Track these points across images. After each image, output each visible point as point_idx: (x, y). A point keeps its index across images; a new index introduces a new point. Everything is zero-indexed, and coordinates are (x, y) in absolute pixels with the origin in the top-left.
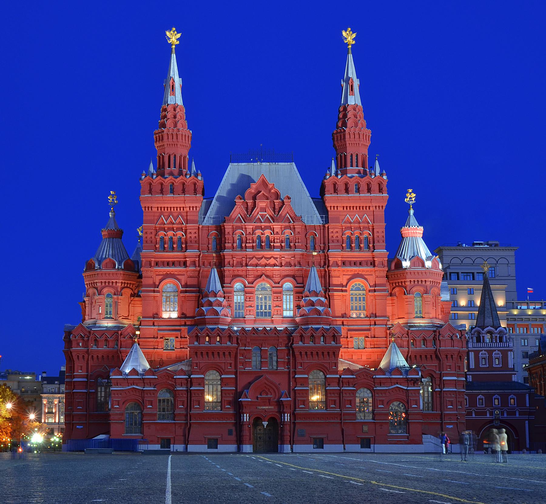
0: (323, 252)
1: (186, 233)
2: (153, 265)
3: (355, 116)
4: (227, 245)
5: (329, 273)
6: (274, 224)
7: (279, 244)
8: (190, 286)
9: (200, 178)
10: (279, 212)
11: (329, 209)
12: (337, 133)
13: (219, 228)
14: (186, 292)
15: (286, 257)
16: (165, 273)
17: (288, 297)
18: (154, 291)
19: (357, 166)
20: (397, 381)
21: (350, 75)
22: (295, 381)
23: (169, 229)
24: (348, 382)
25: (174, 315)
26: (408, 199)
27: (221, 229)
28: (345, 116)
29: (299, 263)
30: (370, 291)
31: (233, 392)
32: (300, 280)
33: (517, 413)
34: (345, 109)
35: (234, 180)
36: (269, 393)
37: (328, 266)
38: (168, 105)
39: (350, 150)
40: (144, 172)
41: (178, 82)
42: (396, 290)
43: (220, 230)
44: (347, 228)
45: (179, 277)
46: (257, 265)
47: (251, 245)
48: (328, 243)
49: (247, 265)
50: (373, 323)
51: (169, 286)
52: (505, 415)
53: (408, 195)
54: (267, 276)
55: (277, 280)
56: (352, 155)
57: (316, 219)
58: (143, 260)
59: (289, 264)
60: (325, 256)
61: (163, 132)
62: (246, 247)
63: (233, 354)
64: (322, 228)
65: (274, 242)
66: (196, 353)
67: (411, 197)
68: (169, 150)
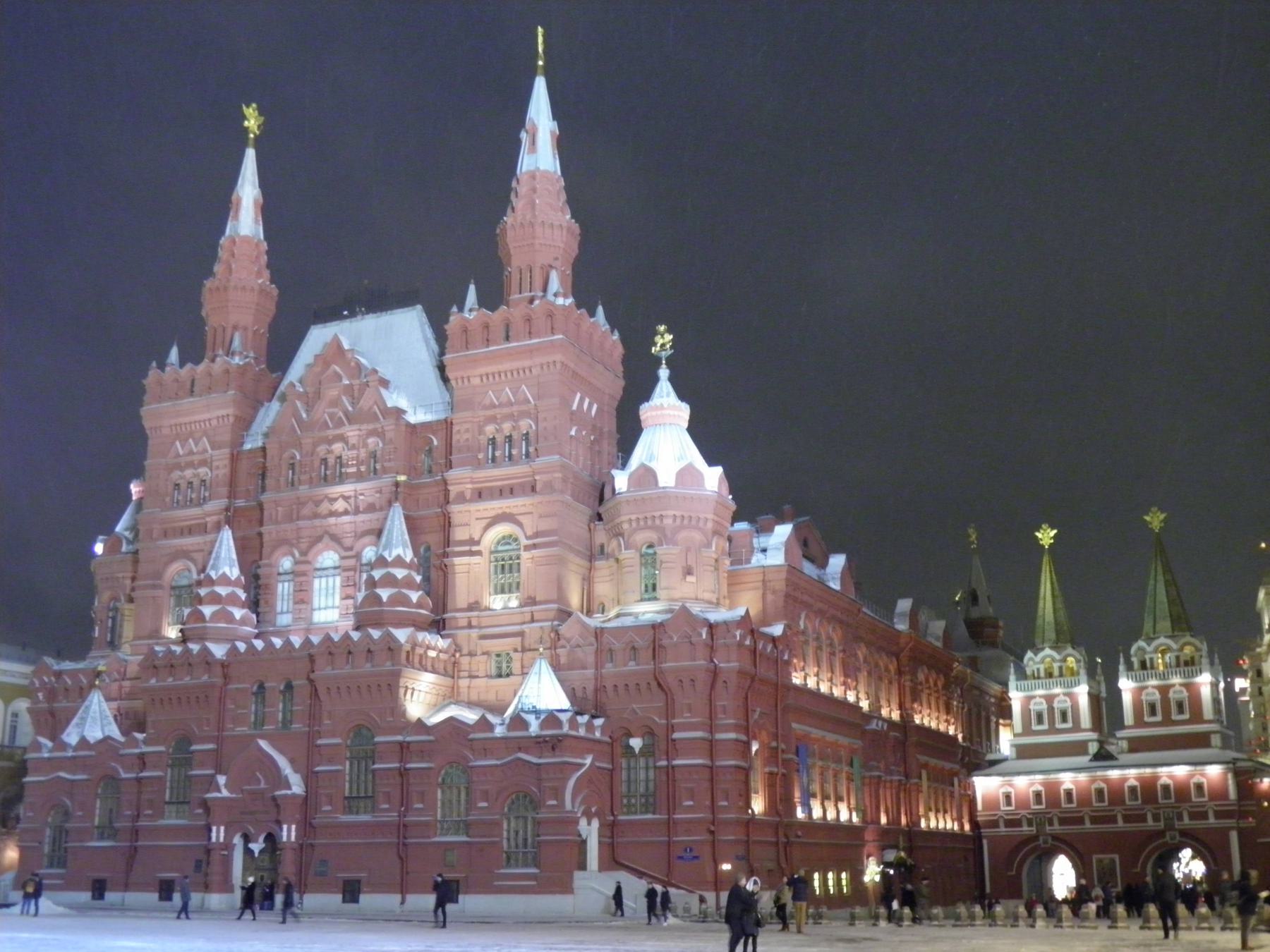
7: (353, 470)
15: (367, 493)
24: (424, 751)
30: (527, 548)
33: (1211, 814)
35: (310, 360)
45: (195, 555)
50: (528, 617)
52: (1186, 820)
53: (659, 340)
54: (336, 539)
55: (348, 542)
59: (371, 508)
67: (664, 340)
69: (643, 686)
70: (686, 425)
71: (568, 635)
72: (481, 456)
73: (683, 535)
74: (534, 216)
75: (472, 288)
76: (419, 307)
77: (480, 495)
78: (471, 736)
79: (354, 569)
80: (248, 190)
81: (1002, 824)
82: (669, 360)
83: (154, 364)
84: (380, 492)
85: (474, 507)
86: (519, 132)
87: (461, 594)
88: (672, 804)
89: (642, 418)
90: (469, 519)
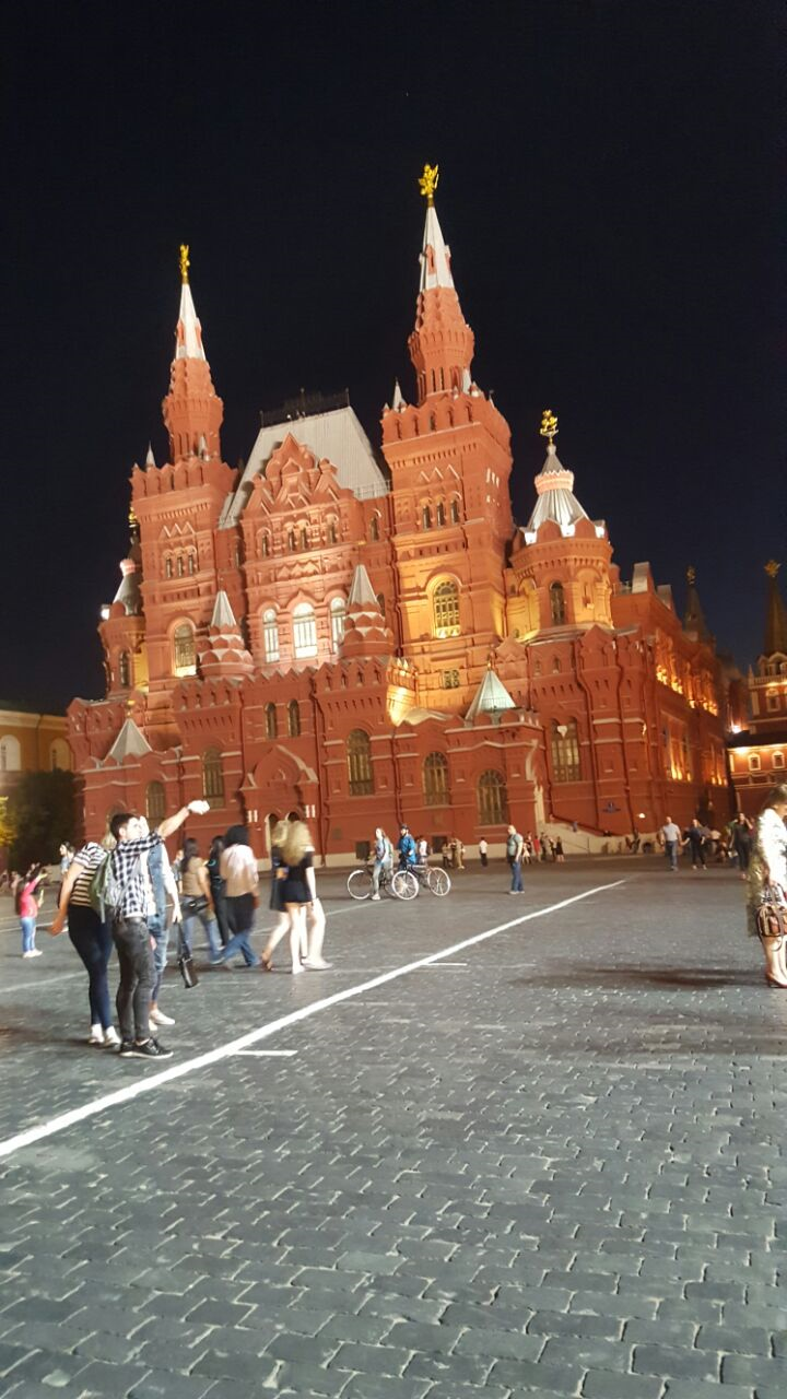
2: (157, 599)
5: (398, 572)
7: (318, 540)
11: (391, 467)
20: (486, 735)
24: (408, 745)
25: (192, 670)
26: (545, 430)
42: (525, 582)
43: (239, 529)
45: (192, 614)
46: (290, 577)
47: (280, 547)
49: (276, 580)
50: (469, 642)
53: (546, 423)
54: (307, 593)
55: (319, 595)
59: (335, 569)
62: (274, 552)
67: (550, 424)
69: (566, 688)
70: (571, 489)
71: (504, 654)
72: (419, 523)
73: (581, 573)
74: (442, 326)
75: (398, 389)
76: (350, 408)
77: (421, 553)
78: (447, 731)
79: (326, 615)
80: (189, 319)
81: (750, 780)
83: (136, 466)
84: (341, 555)
85: (416, 563)
86: (418, 257)
87: (414, 629)
88: (595, 775)
89: (537, 486)
90: (414, 572)
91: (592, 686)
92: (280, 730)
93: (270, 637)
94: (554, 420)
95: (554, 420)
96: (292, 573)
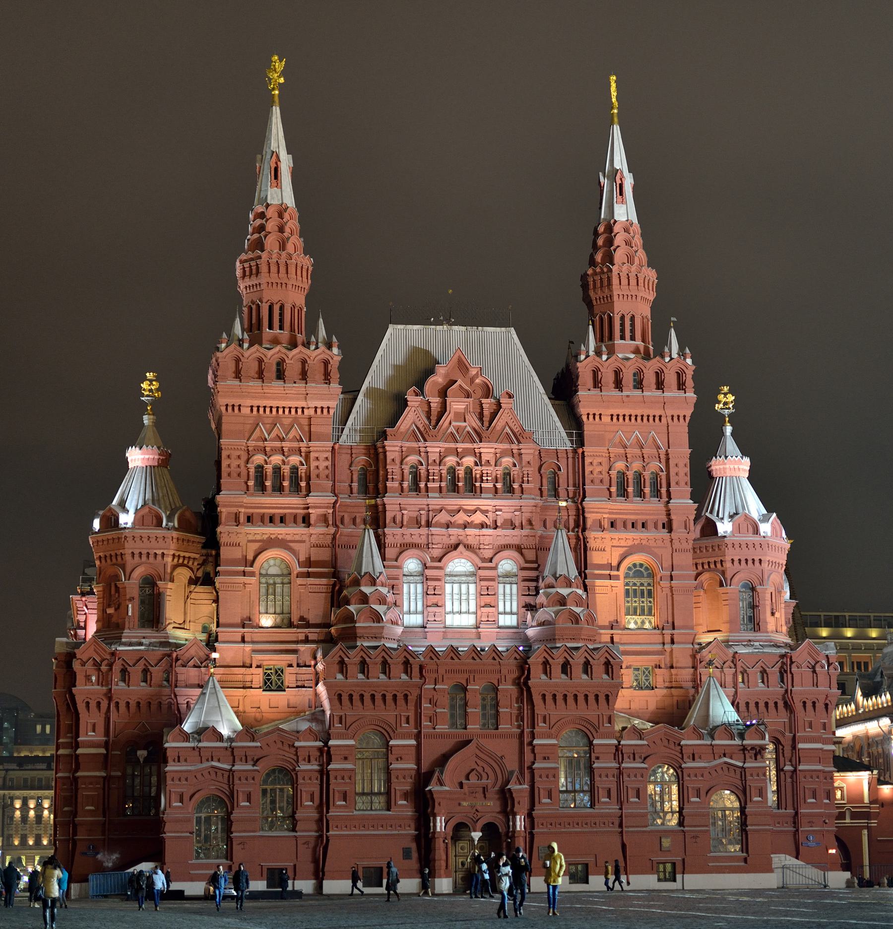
0: (574, 502)
1: (307, 458)
3: (628, 243)
4: (389, 484)
6: (481, 445)
7: (490, 485)
8: (318, 564)
9: (335, 350)
10: (491, 423)
11: (584, 418)
12: (595, 273)
13: (372, 451)
14: (308, 575)
16: (265, 537)
17: (508, 586)
18: (244, 574)
19: (633, 338)
21: (617, 166)
22: (533, 751)
23: (275, 451)
27: (377, 454)
28: (610, 242)
29: (530, 522)
31: (413, 773)
32: (531, 555)
34: (609, 228)
35: (400, 359)
36: (484, 775)
37: (584, 530)
38: (268, 206)
39: (620, 307)
40: (224, 336)
41: (286, 162)
44: (618, 457)
47: (437, 485)
48: (584, 484)
49: (428, 524)
51: (271, 561)
53: (721, 397)
54: (468, 547)
55: (488, 554)
56: (623, 318)
57: (559, 438)
58: (223, 510)
59: (511, 524)
60: (578, 509)
61: (260, 257)
63: (412, 698)
64: (570, 455)
65: (482, 481)
66: (340, 696)
67: (726, 400)
68: (271, 295)
69: (771, 705)
77: (612, 525)
79: (493, 580)
82: (733, 419)
84: (520, 510)
85: (607, 535)
90: (605, 547)
91: (798, 706)
92: (470, 718)
93: (412, 594)
94: (731, 398)
95: (731, 398)
96: (453, 520)
